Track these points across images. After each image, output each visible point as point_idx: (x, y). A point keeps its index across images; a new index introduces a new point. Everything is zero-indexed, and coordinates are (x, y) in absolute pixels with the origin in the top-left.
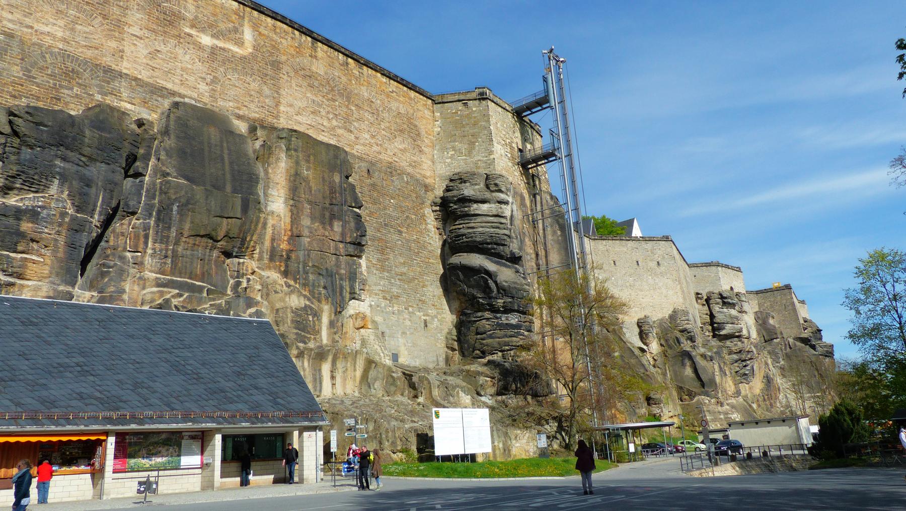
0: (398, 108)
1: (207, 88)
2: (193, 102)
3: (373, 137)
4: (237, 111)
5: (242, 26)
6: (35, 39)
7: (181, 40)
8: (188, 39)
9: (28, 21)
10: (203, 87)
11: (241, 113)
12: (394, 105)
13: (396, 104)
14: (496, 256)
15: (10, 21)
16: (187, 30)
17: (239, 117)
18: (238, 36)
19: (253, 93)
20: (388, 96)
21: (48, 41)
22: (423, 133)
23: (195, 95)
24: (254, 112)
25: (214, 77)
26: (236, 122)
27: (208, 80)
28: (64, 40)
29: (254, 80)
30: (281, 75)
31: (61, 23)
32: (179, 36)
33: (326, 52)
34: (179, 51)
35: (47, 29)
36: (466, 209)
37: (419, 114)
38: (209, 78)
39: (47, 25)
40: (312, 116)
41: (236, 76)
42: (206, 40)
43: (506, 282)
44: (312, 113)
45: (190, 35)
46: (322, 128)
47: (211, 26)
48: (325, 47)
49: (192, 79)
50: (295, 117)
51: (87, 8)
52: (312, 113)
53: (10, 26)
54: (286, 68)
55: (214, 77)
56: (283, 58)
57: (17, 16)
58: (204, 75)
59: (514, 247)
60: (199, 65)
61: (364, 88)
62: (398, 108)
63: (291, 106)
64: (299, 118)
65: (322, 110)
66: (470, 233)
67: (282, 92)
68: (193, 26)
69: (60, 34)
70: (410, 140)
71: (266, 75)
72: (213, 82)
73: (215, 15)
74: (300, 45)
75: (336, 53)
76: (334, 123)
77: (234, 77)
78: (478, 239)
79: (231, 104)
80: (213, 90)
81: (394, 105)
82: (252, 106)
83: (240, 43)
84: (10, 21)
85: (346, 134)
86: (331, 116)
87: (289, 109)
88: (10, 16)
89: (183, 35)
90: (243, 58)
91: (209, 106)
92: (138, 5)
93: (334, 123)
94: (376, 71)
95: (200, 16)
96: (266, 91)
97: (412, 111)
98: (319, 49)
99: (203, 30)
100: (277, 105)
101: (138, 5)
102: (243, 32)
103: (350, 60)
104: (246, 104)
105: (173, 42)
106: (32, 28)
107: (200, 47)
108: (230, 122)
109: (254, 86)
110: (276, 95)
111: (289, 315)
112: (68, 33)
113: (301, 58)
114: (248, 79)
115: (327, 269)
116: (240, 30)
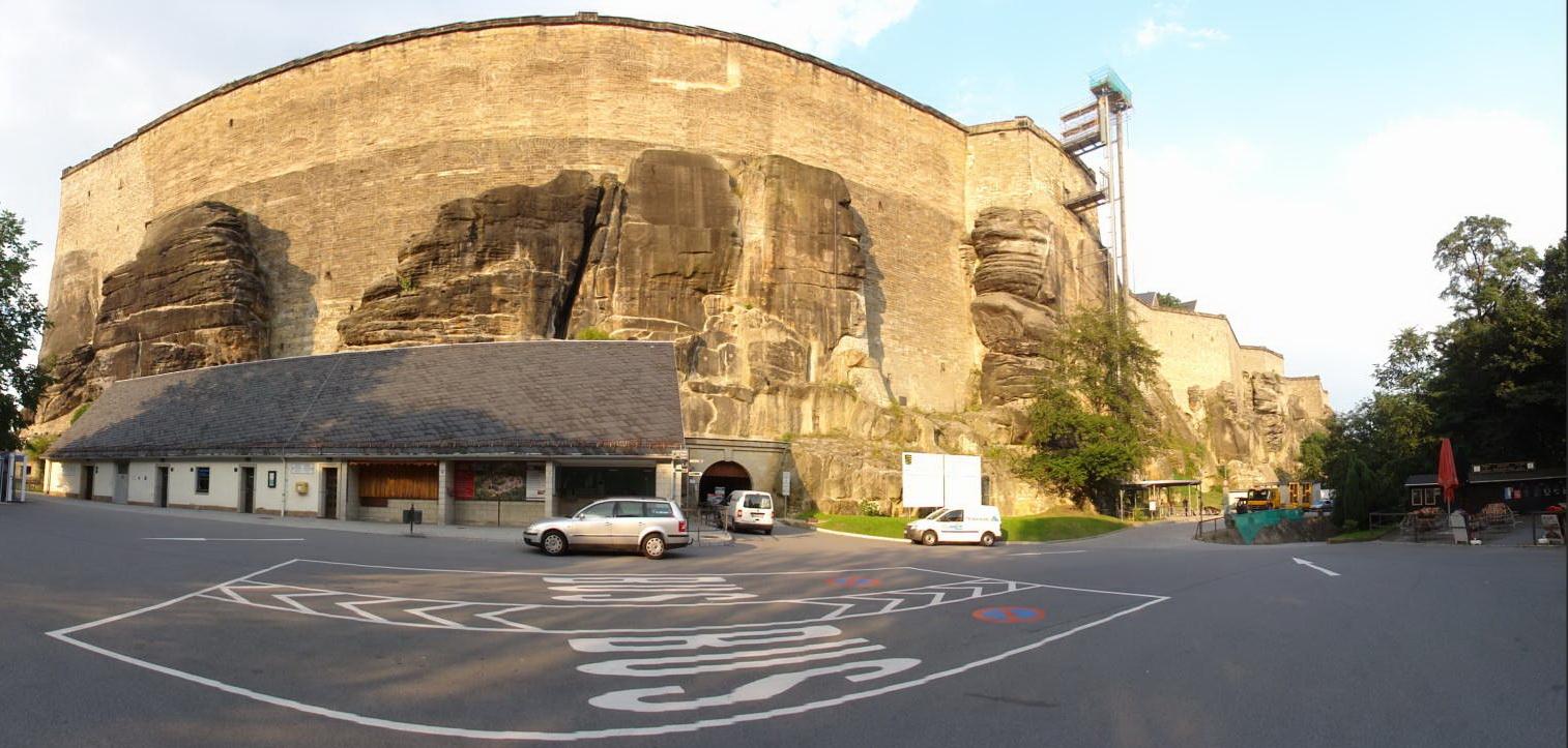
0: (920, 138)
1: (683, 133)
2: (670, 149)
3: (887, 167)
4: (721, 150)
5: (724, 62)
6: (510, 137)
7: (649, 92)
8: (656, 89)
9: (500, 124)
10: (680, 133)
11: (725, 151)
12: (915, 135)
13: (918, 134)
14: (1029, 298)
15: (486, 130)
16: (655, 80)
17: (722, 155)
18: (720, 73)
19: (740, 129)
20: (908, 125)
21: (520, 133)
22: (951, 165)
23: (671, 142)
24: (742, 149)
25: (691, 120)
26: (718, 160)
27: (685, 124)
28: (534, 128)
29: (741, 116)
30: (774, 106)
31: (529, 114)
32: (647, 88)
33: (830, 79)
34: (647, 103)
35: (516, 124)
36: (994, 246)
37: (948, 146)
38: (685, 123)
39: (518, 120)
40: (812, 147)
41: (719, 114)
42: (681, 85)
43: (1032, 323)
44: (812, 143)
45: (657, 85)
46: (825, 159)
47: (685, 70)
48: (829, 73)
49: (668, 126)
50: (791, 149)
51: (551, 92)
52: (812, 143)
53: (488, 133)
54: (779, 99)
55: (691, 120)
56: (777, 88)
57: (493, 122)
58: (680, 121)
59: (1049, 291)
60: (675, 112)
61: (877, 116)
62: (920, 138)
63: (785, 137)
64: (795, 150)
65: (823, 139)
66: (996, 271)
67: (774, 123)
68: (659, 75)
69: (529, 124)
70: (935, 173)
71: (756, 108)
72: (689, 125)
73: (689, 59)
74: (797, 72)
75: (844, 78)
76: (839, 153)
77: (716, 116)
78: (1004, 277)
79: (714, 143)
80: (690, 133)
81: (915, 135)
82: (740, 142)
83: (723, 80)
84: (486, 130)
85: (853, 164)
86: (834, 146)
87: (783, 141)
88: (486, 126)
89: (650, 86)
90: (727, 96)
91: (686, 150)
92: (598, 71)
93: (839, 153)
94: (894, 96)
95: (674, 63)
96: (756, 124)
97: (939, 142)
98: (821, 75)
99: (677, 76)
100: (767, 138)
101: (598, 71)
102: (726, 68)
103: (861, 85)
104: (730, 141)
105: (640, 96)
106: (507, 127)
107: (675, 94)
108: (713, 160)
109: (742, 121)
110: (766, 128)
111: (764, 350)
112: (535, 120)
113: (798, 87)
114: (734, 115)
115: (815, 303)
116: (723, 68)
